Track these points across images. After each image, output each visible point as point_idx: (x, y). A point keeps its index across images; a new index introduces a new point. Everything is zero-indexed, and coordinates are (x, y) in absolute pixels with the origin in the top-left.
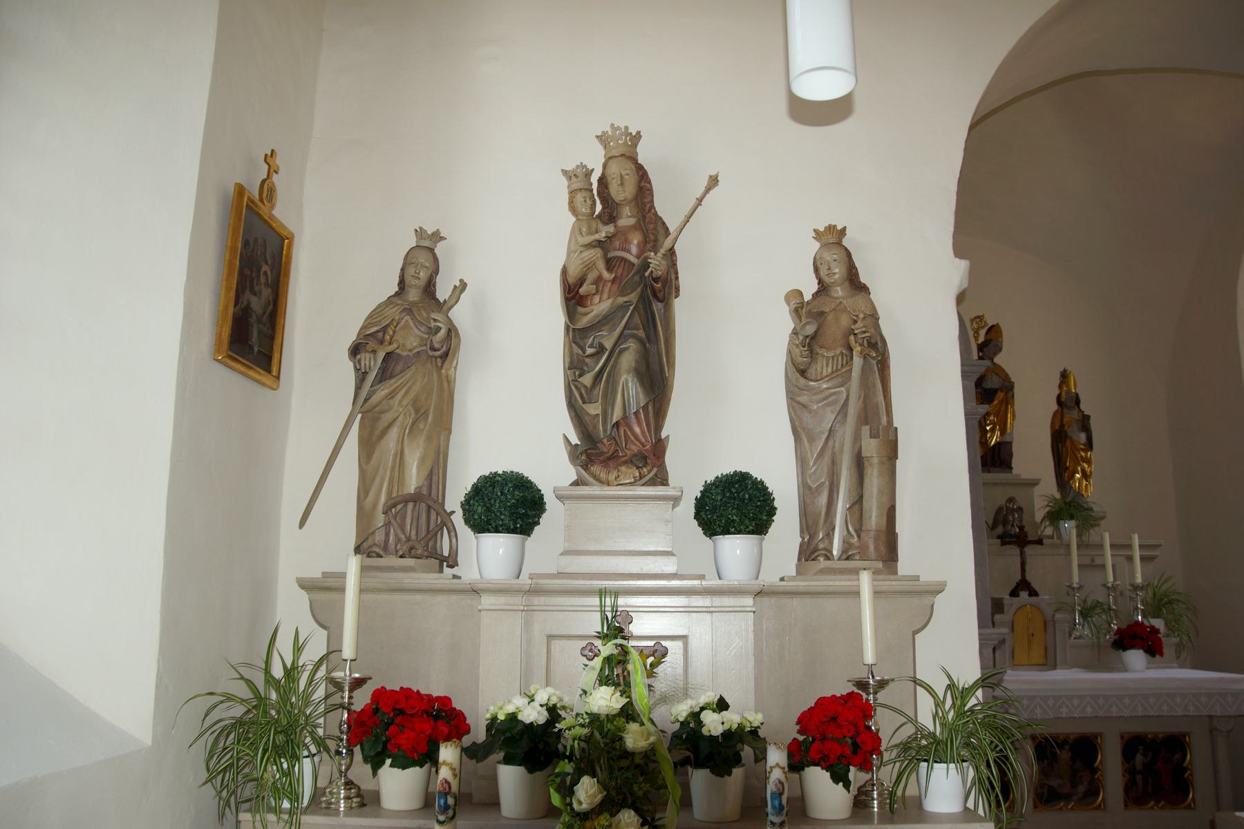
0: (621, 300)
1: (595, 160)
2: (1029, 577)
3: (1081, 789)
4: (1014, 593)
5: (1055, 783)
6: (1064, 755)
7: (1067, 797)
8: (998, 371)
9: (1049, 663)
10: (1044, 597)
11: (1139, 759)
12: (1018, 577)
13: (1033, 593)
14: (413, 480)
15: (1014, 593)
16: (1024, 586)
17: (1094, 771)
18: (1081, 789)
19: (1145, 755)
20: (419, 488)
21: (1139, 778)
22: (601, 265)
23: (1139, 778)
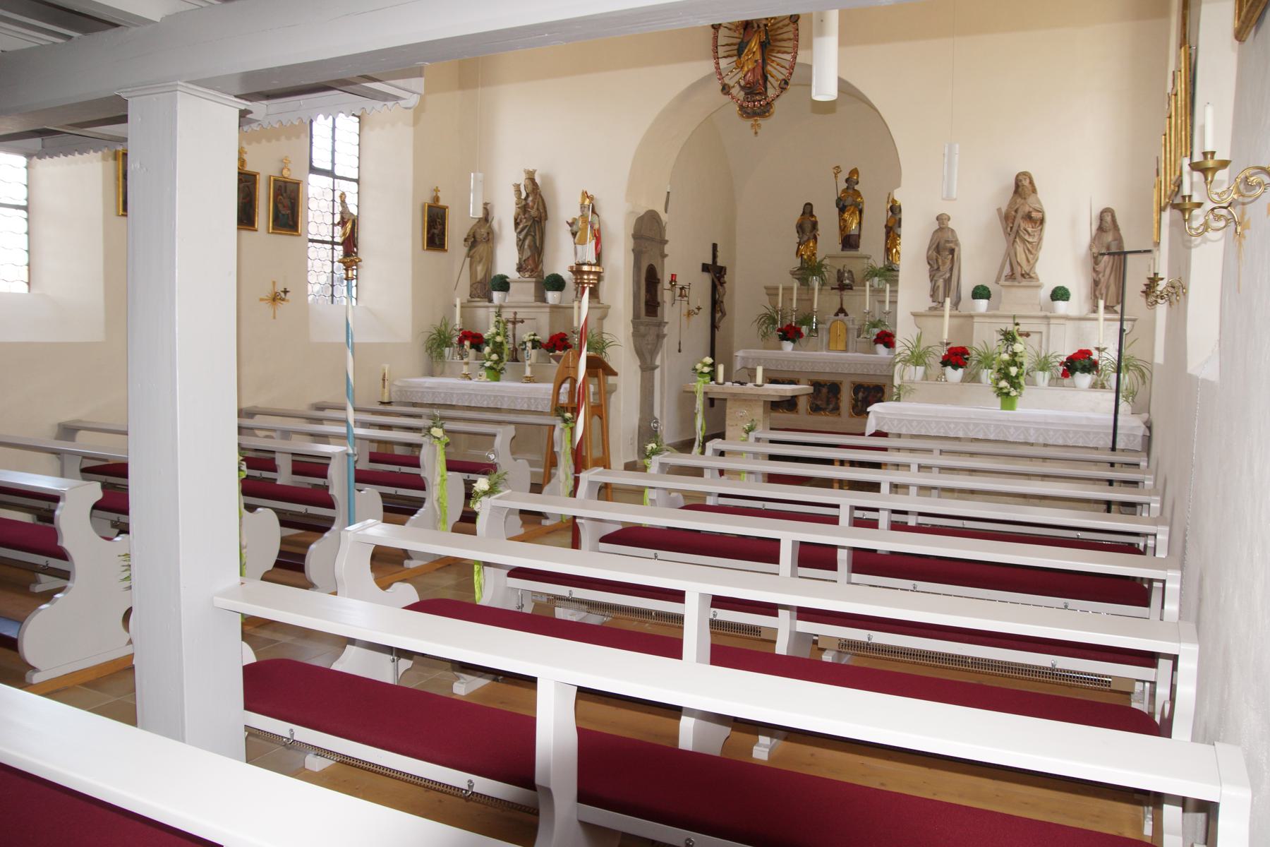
0: (525, 224)
1: (522, 180)
2: (844, 307)
3: (831, 406)
4: (837, 315)
5: (819, 403)
6: (824, 390)
7: (824, 410)
8: (858, 194)
9: (846, 351)
10: (851, 316)
11: (860, 395)
12: (839, 306)
13: (846, 315)
14: (480, 276)
15: (837, 315)
16: (842, 310)
17: (838, 399)
18: (831, 406)
19: (863, 393)
20: (481, 280)
21: (859, 403)
22: (521, 214)
23: (859, 403)
